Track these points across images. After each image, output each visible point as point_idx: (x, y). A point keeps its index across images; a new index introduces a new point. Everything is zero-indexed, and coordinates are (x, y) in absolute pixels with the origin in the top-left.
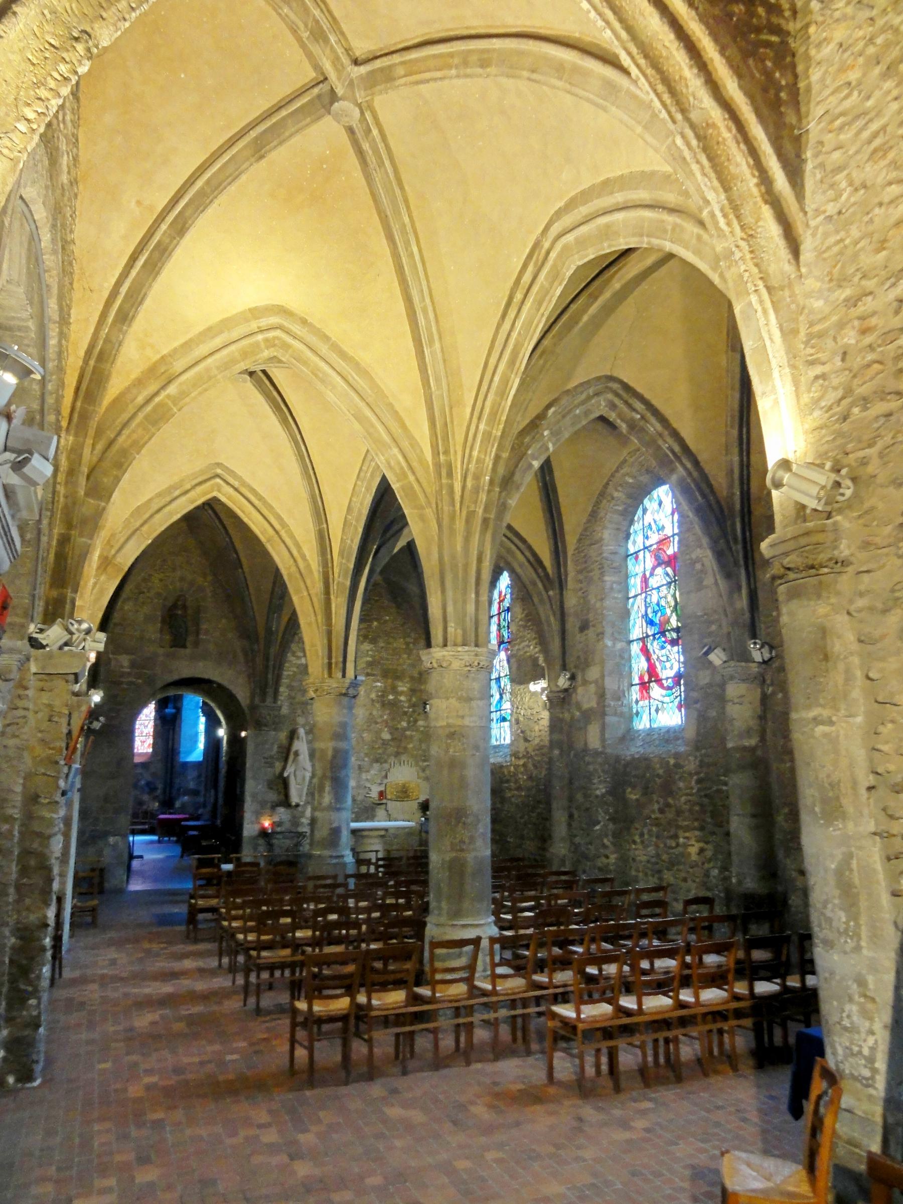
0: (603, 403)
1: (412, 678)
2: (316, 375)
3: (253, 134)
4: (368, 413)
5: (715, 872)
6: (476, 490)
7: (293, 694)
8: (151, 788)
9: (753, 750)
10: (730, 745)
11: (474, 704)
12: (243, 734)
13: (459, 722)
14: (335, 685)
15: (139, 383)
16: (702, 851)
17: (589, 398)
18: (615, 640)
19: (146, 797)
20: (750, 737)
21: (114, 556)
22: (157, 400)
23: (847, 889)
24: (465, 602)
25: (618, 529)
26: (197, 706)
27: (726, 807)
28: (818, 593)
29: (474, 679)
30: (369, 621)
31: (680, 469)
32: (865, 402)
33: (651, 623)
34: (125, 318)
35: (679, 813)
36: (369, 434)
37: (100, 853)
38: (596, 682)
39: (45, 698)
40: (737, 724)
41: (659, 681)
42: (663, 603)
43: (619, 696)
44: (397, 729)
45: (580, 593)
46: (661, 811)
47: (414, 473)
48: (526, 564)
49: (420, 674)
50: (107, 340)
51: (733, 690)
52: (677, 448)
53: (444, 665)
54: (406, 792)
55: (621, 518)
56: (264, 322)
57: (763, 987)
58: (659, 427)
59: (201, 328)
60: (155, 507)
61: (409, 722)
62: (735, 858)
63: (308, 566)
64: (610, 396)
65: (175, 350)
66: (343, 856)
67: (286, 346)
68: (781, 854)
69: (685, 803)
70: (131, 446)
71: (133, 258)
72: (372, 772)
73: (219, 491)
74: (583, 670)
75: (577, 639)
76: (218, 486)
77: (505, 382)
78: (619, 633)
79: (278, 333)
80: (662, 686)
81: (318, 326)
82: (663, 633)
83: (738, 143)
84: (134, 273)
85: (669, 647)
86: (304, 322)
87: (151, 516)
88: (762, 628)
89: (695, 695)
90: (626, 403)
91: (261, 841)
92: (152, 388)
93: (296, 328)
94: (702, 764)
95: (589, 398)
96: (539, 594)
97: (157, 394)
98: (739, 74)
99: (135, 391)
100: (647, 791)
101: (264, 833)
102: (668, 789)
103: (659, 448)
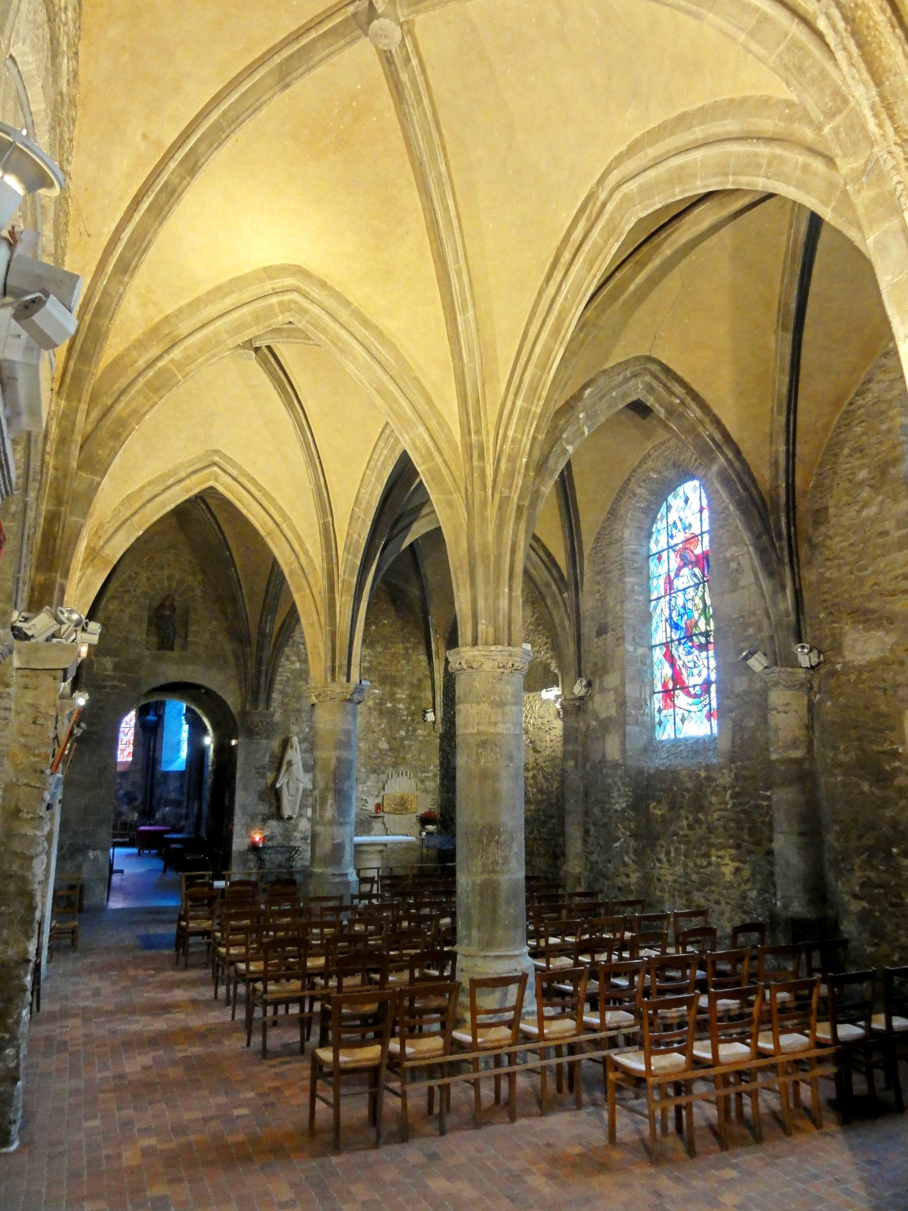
0: (641, 386)
1: (412, 685)
2: (335, 345)
3: (277, 59)
4: (392, 388)
5: (754, 894)
6: (511, 474)
7: (286, 700)
8: (129, 798)
9: (798, 762)
10: (774, 757)
11: (508, 709)
12: (233, 742)
13: (492, 730)
14: (339, 690)
15: (140, 344)
16: (737, 870)
17: (626, 380)
18: (636, 645)
19: (125, 808)
20: (797, 748)
21: (102, 547)
22: (160, 364)
24: (497, 597)
25: (639, 528)
26: (180, 714)
27: (770, 825)
29: (507, 683)
31: (722, 459)
33: (676, 627)
34: (125, 268)
35: (711, 829)
36: (393, 410)
37: (79, 867)
38: (615, 689)
39: (29, 696)
40: (782, 734)
41: (685, 689)
42: (689, 605)
43: (641, 704)
44: (395, 739)
45: (598, 595)
46: (690, 827)
47: (441, 454)
48: (540, 564)
49: (420, 680)
50: (105, 292)
51: (776, 697)
52: (718, 437)
53: (475, 665)
55: (643, 516)
56: (280, 283)
57: (848, 1031)
58: (699, 413)
59: (210, 287)
60: (147, 495)
62: (779, 880)
63: (311, 562)
64: (648, 378)
65: (180, 310)
66: (346, 875)
67: (303, 311)
68: (831, 876)
69: (718, 820)
70: (130, 415)
71: (137, 201)
72: (369, 783)
73: (216, 480)
74: (601, 677)
75: (594, 645)
76: (215, 474)
77: (548, 352)
78: (641, 638)
79: (294, 296)
80: (688, 694)
81: (339, 290)
82: (689, 637)
83: (893, 27)
84: (137, 217)
85: (696, 652)
86: (323, 284)
87: (143, 505)
88: (807, 631)
89: (729, 702)
90: (665, 386)
91: (251, 856)
92: (155, 351)
93: (314, 292)
94: (737, 778)
95: (626, 380)
96: (553, 596)
97: (160, 357)
99: (134, 353)
100: (673, 806)
101: (254, 848)
102: (698, 803)
103: (699, 435)
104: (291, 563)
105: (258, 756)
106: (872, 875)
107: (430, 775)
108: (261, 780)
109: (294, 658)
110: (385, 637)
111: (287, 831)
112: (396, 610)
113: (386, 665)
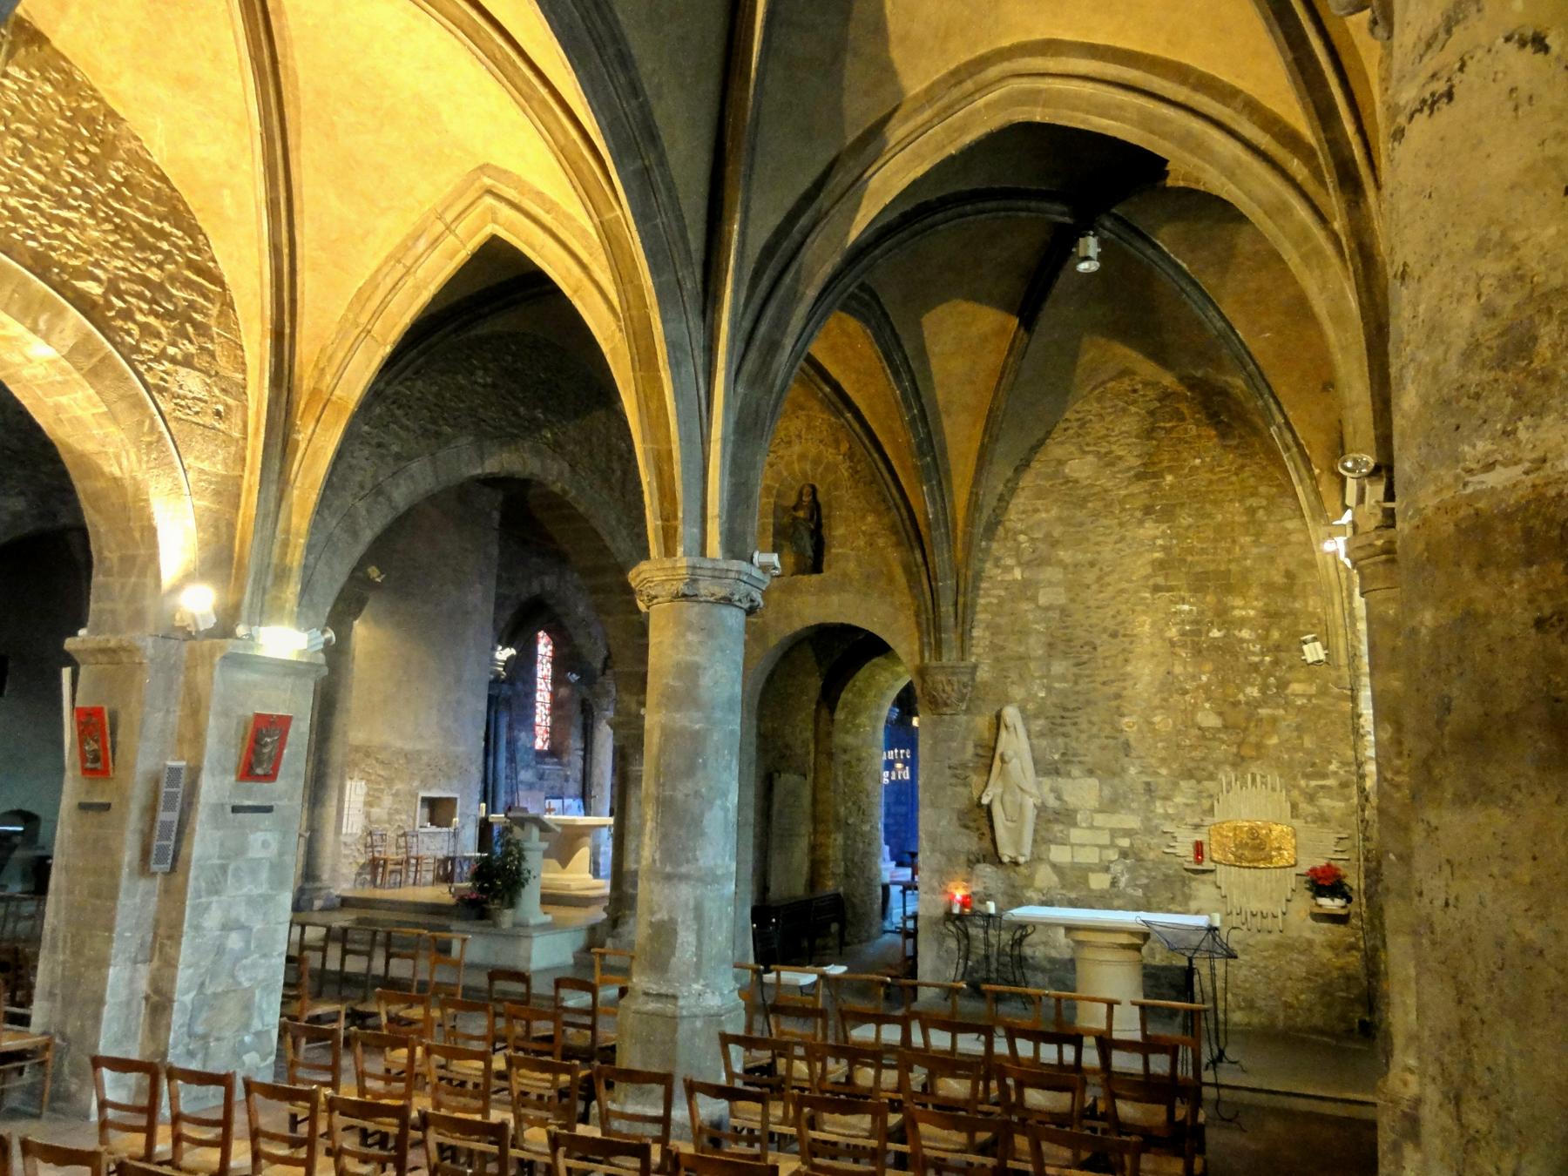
7: (999, 640)
30: (1155, 475)
44: (1236, 704)
48: (1245, 157)
49: (1289, 575)
54: (1260, 847)
61: (1264, 688)
66: (675, 997)
72: (1179, 799)
73: (495, 221)
96: (1305, 236)
104: (613, 335)
105: (954, 745)
107: (1331, 782)
108: (960, 789)
109: (1010, 562)
110: (1196, 495)
111: (1013, 887)
112: (1223, 436)
113: (1203, 551)
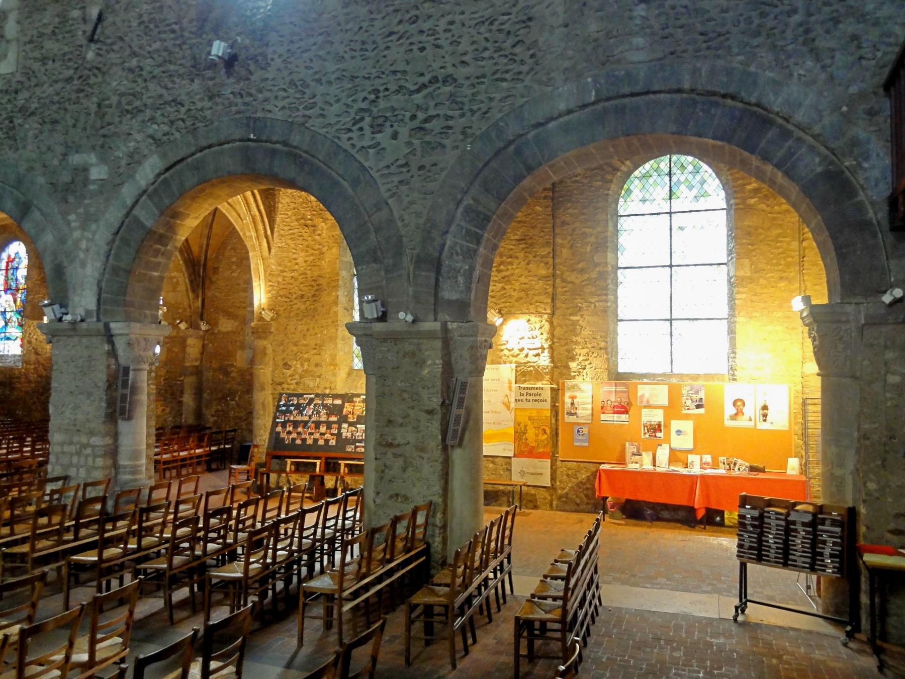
9: (197, 367)
10: (187, 364)
16: (164, 410)
23: (263, 405)
28: (265, 338)
32: (281, 296)
40: (191, 356)
51: (190, 341)
57: (213, 448)
62: (184, 412)
68: (204, 410)
88: (205, 315)
98: (263, 203)
106: (220, 408)
